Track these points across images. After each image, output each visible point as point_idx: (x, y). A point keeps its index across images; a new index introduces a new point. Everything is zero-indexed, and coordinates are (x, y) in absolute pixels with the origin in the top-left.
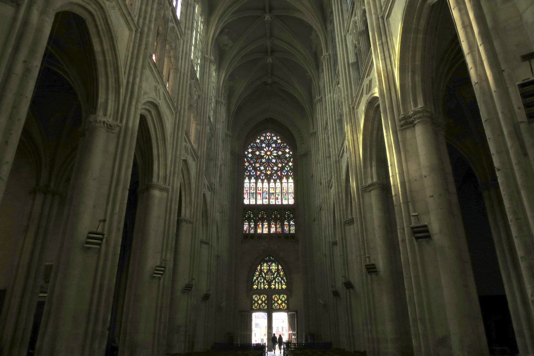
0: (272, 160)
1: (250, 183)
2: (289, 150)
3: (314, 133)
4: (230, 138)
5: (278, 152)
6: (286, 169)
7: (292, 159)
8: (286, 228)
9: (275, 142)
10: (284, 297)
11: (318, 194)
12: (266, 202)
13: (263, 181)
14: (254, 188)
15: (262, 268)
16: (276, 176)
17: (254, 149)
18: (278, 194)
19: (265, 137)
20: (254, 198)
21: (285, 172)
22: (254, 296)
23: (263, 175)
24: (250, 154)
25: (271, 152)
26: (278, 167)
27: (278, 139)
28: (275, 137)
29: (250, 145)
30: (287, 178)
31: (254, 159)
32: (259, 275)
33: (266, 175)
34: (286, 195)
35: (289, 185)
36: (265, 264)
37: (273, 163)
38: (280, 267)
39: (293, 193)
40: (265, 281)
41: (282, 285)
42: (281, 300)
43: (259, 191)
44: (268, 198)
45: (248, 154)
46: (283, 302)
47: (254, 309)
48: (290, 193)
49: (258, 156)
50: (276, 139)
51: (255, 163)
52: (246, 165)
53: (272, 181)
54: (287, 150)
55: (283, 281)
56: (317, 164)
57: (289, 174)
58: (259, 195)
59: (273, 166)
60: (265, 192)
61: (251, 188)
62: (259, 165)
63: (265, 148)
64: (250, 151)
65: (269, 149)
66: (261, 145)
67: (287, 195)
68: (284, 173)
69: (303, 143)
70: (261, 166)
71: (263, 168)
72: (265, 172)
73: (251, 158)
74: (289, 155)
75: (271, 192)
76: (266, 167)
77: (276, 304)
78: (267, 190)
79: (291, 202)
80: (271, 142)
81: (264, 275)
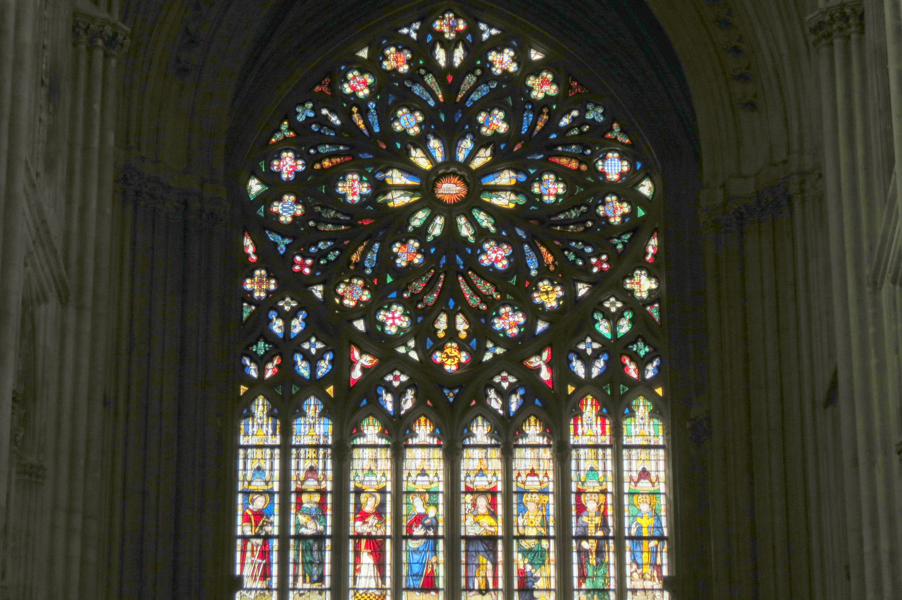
0: (477, 248)
1: (286, 449)
2: (625, 166)
3: (845, 18)
4: (113, 62)
5: (531, 180)
6: (603, 327)
7: (654, 242)
11: (884, 545)
14: (323, 493)
16: (513, 390)
17: (320, 158)
18: (532, 543)
20: (321, 579)
21: (596, 355)
26: (534, 312)
27: (529, 68)
28: (508, 54)
29: (290, 116)
31: (326, 237)
34: (600, 552)
37: (489, 274)
39: (661, 538)
43: (363, 516)
44: (441, 583)
45: (266, 199)
48: (639, 538)
50: (513, 68)
52: (248, 297)
53: (481, 432)
56: (876, 286)
57: (632, 371)
58: (367, 559)
59: (484, 298)
60: (418, 531)
61: (293, 498)
62: (366, 296)
63: (421, 142)
65: (450, 149)
66: (387, 115)
67: (611, 558)
68: (588, 362)
69: (751, 106)
70: (380, 300)
71: (405, 323)
72: (414, 355)
74: (626, 208)
75: (469, 528)
76: (431, 314)
78: (438, 512)
80: (476, 96)
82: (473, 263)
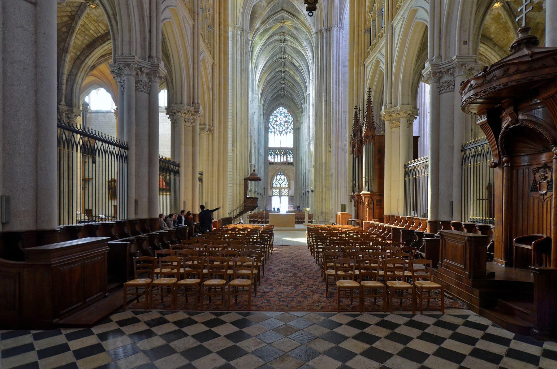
8: (289, 159)
9: (284, 113)
10: (287, 190)
33: (279, 131)
38: (285, 177)
51: (274, 124)
54: (290, 118)
77: (283, 193)
79: (292, 146)
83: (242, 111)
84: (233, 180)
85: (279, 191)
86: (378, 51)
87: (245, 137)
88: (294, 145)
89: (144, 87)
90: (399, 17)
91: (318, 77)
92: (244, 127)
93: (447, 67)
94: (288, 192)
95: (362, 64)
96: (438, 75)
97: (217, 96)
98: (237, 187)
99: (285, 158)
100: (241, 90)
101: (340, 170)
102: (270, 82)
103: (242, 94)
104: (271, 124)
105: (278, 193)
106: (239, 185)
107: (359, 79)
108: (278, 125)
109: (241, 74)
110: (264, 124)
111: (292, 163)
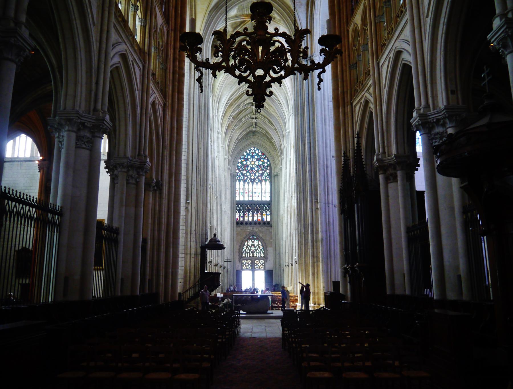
6: (265, 175)
8: (264, 217)
9: (257, 155)
12: (250, 199)
13: (248, 183)
15: (248, 243)
19: (250, 151)
22: (243, 261)
23: (248, 179)
24: (240, 164)
25: (254, 162)
26: (259, 174)
30: (266, 181)
32: (246, 248)
33: (251, 179)
35: (266, 186)
36: (250, 241)
37: (255, 170)
38: (260, 243)
40: (250, 252)
41: (261, 254)
42: (260, 263)
46: (262, 265)
47: (243, 269)
49: (245, 165)
51: (243, 170)
54: (266, 161)
55: (261, 252)
57: (267, 178)
63: (250, 159)
64: (239, 162)
66: (247, 156)
73: (241, 167)
74: (267, 165)
76: (251, 174)
77: (257, 266)
81: (249, 248)
82: (254, 169)
83: (200, 157)
84: (186, 248)
85: (252, 263)
86: (366, 90)
87: (203, 190)
88: (271, 197)
89: (86, 143)
90: (385, 56)
91: (298, 114)
92: (202, 177)
93: (436, 118)
94: (264, 263)
95: (349, 104)
96: (427, 125)
97: (168, 142)
98: (192, 258)
99: (259, 215)
100: (199, 130)
101: (332, 234)
102: (237, 116)
103: (200, 136)
104: (238, 169)
105: (249, 266)
106: (194, 256)
107: (346, 120)
108: (249, 170)
109: (199, 112)
110: (229, 171)
111: (269, 223)
